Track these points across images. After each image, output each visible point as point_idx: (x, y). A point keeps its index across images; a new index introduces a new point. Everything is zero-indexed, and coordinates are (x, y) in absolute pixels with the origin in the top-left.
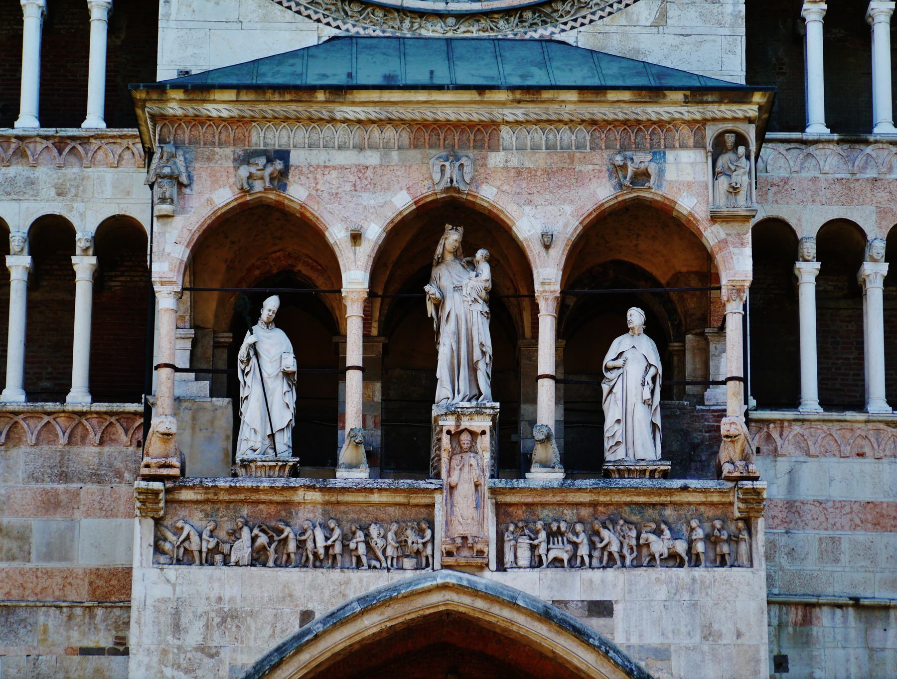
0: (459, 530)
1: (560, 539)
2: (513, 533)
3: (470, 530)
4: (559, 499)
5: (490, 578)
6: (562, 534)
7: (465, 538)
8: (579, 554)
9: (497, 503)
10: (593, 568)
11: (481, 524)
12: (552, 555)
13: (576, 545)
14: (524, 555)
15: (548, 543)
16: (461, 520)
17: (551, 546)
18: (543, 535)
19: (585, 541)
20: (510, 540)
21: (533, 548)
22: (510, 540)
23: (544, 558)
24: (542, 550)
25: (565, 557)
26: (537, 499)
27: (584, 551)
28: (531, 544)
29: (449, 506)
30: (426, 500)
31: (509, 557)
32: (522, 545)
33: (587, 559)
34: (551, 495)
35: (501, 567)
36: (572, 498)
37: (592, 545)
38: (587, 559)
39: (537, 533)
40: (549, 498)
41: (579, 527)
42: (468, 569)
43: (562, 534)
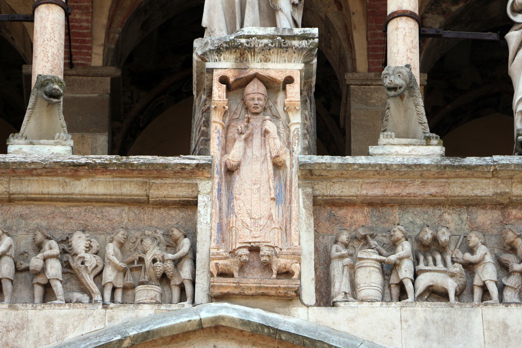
0: (244, 235)
1: (438, 257)
2: (346, 246)
3: (269, 237)
4: (433, 190)
5: (302, 318)
6: (442, 249)
7: (255, 250)
8: (477, 282)
9: (315, 197)
10: (508, 304)
11: (286, 230)
12: (424, 281)
13: (470, 267)
14: (370, 279)
15: (416, 262)
16: (248, 221)
17: (422, 266)
18: (405, 248)
19: (489, 258)
20: (342, 257)
21: (388, 270)
22: (342, 257)
23: (409, 286)
24: (406, 271)
25: (451, 286)
26: (392, 191)
27: (488, 273)
28: (381, 262)
29: (224, 199)
30: (178, 191)
31: (340, 285)
32: (365, 263)
33: (493, 289)
34: (418, 182)
35: (325, 298)
36: (459, 189)
37: (503, 267)
38: (493, 289)
39: (393, 246)
40: (413, 189)
41: (474, 239)
42: (262, 301)
43: (442, 249)
